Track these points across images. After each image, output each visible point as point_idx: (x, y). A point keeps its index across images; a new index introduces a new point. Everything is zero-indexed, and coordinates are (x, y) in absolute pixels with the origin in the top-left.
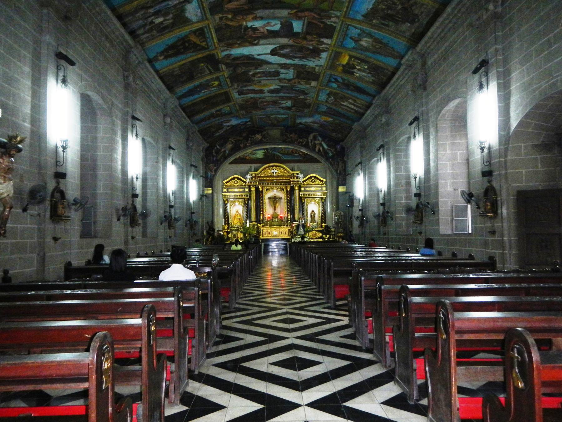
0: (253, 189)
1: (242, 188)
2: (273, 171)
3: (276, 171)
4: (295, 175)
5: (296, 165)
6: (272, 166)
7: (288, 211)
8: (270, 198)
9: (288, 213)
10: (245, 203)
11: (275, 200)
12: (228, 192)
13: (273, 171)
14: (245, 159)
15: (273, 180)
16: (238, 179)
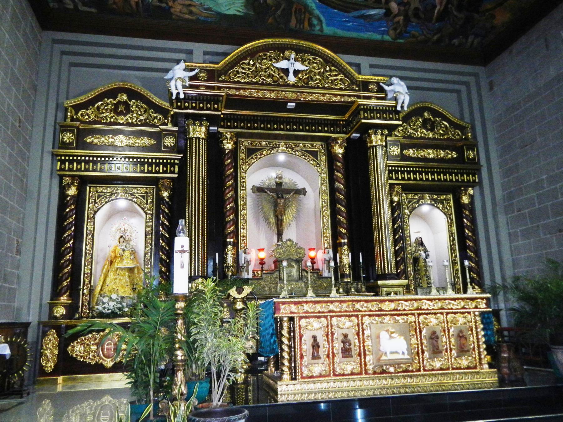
0: (198, 132)
1: (150, 135)
2: (283, 64)
3: (299, 66)
4: (371, 86)
5: (364, 61)
6: (282, 49)
7: (335, 235)
8: (259, 190)
9: (336, 247)
10: (159, 200)
11: (279, 197)
12: (81, 144)
13: (283, 64)
14: (166, 12)
15: (280, 105)
16: (133, 94)
